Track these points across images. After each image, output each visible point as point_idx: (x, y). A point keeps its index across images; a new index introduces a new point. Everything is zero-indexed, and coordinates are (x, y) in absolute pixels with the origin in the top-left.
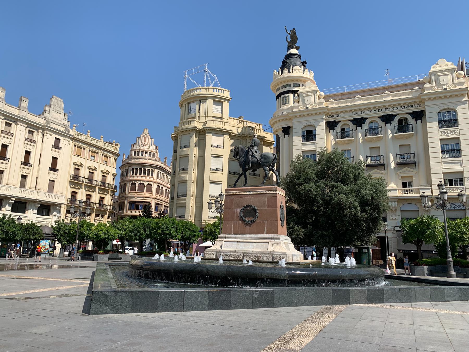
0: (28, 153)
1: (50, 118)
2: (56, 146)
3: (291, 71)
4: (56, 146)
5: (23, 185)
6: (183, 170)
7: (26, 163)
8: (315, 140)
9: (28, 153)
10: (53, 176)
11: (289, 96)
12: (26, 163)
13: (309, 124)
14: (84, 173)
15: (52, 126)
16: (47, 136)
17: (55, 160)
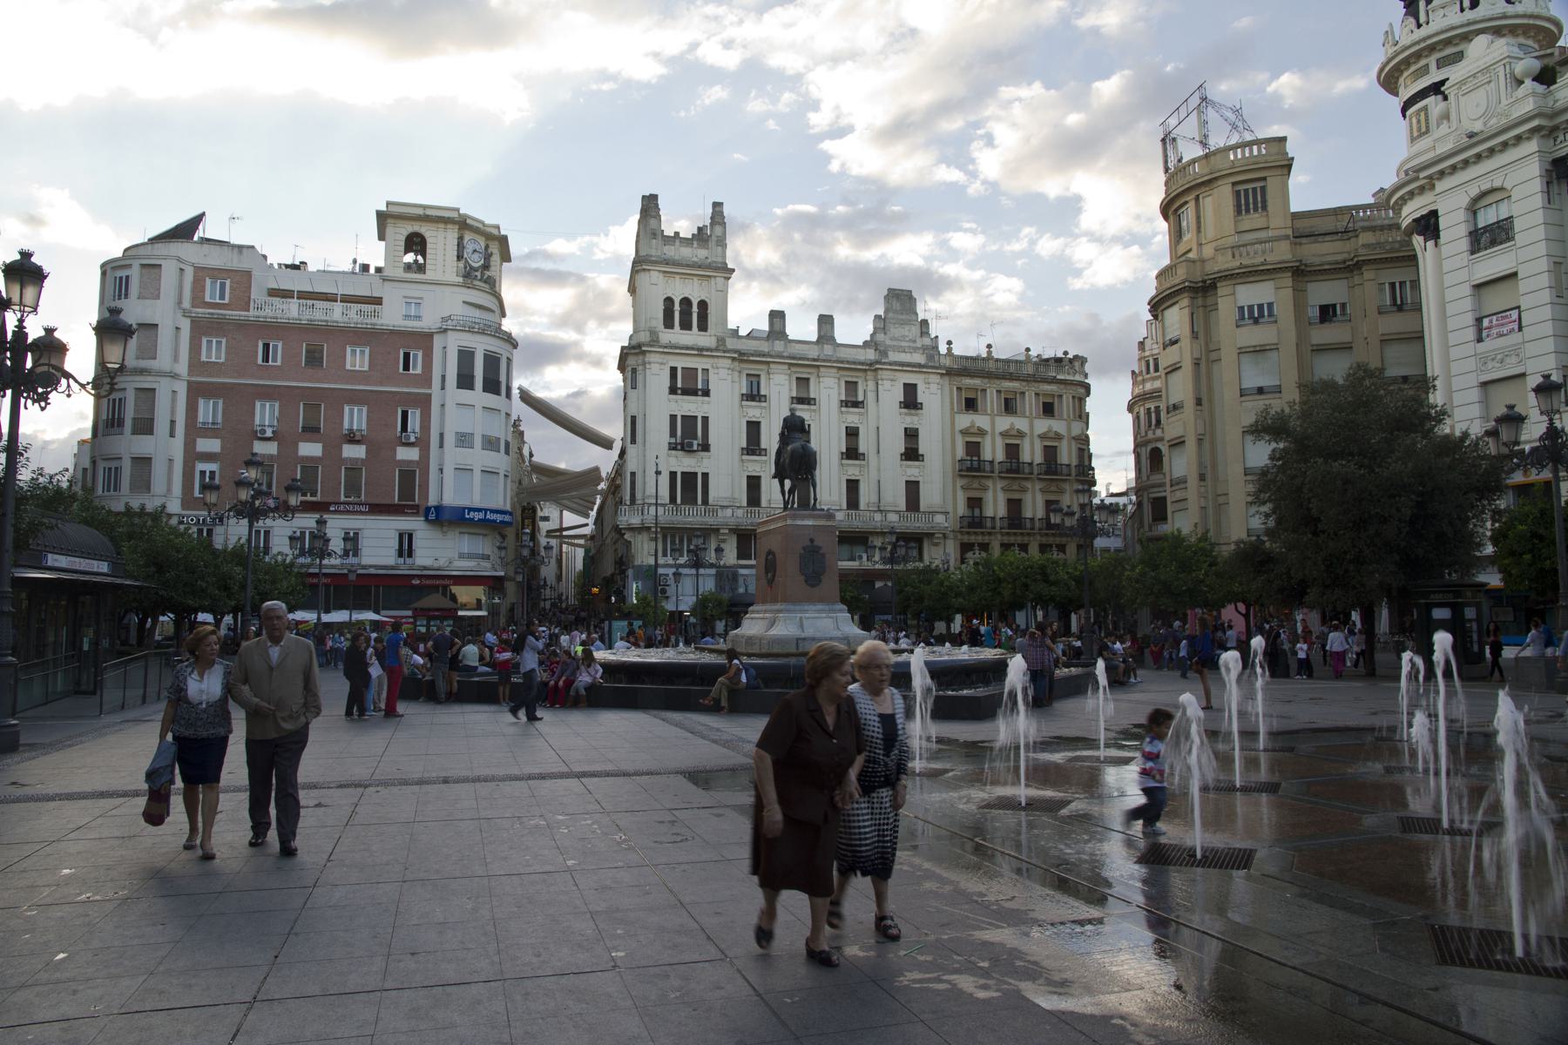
0: (852, 433)
1: (888, 342)
2: (910, 401)
3: (1422, 19)
4: (910, 401)
5: (853, 503)
6: (1175, 407)
7: (852, 453)
8: (1513, 239)
9: (852, 433)
10: (913, 471)
11: (1425, 108)
12: (852, 453)
13: (1486, 186)
14: (993, 451)
15: (894, 356)
16: (885, 385)
17: (911, 435)
